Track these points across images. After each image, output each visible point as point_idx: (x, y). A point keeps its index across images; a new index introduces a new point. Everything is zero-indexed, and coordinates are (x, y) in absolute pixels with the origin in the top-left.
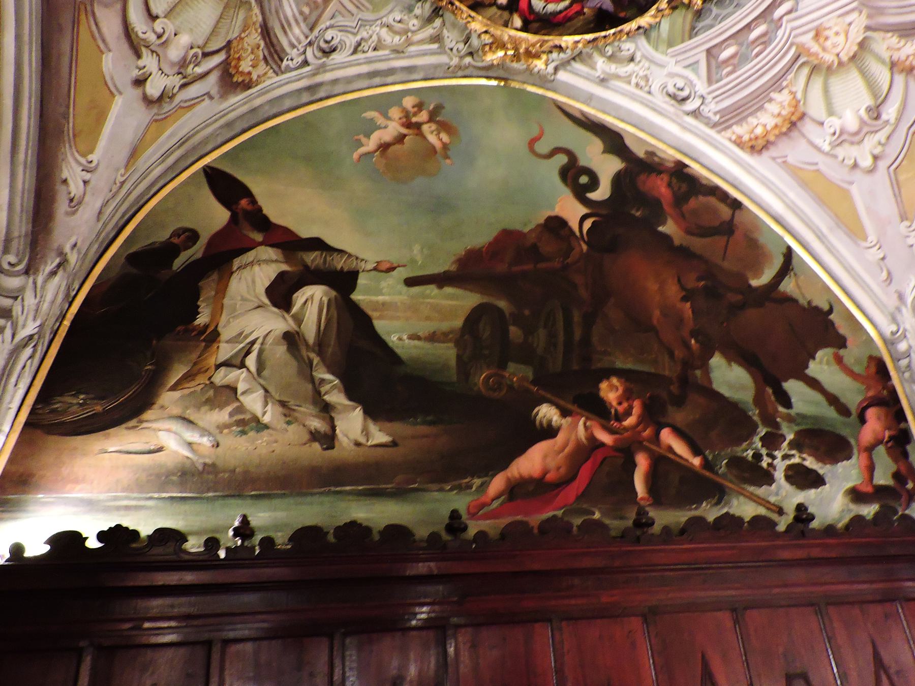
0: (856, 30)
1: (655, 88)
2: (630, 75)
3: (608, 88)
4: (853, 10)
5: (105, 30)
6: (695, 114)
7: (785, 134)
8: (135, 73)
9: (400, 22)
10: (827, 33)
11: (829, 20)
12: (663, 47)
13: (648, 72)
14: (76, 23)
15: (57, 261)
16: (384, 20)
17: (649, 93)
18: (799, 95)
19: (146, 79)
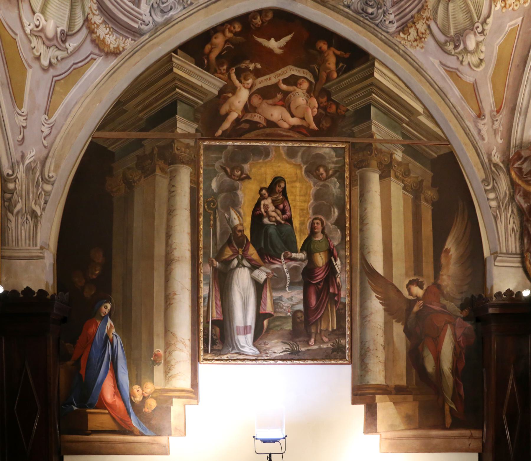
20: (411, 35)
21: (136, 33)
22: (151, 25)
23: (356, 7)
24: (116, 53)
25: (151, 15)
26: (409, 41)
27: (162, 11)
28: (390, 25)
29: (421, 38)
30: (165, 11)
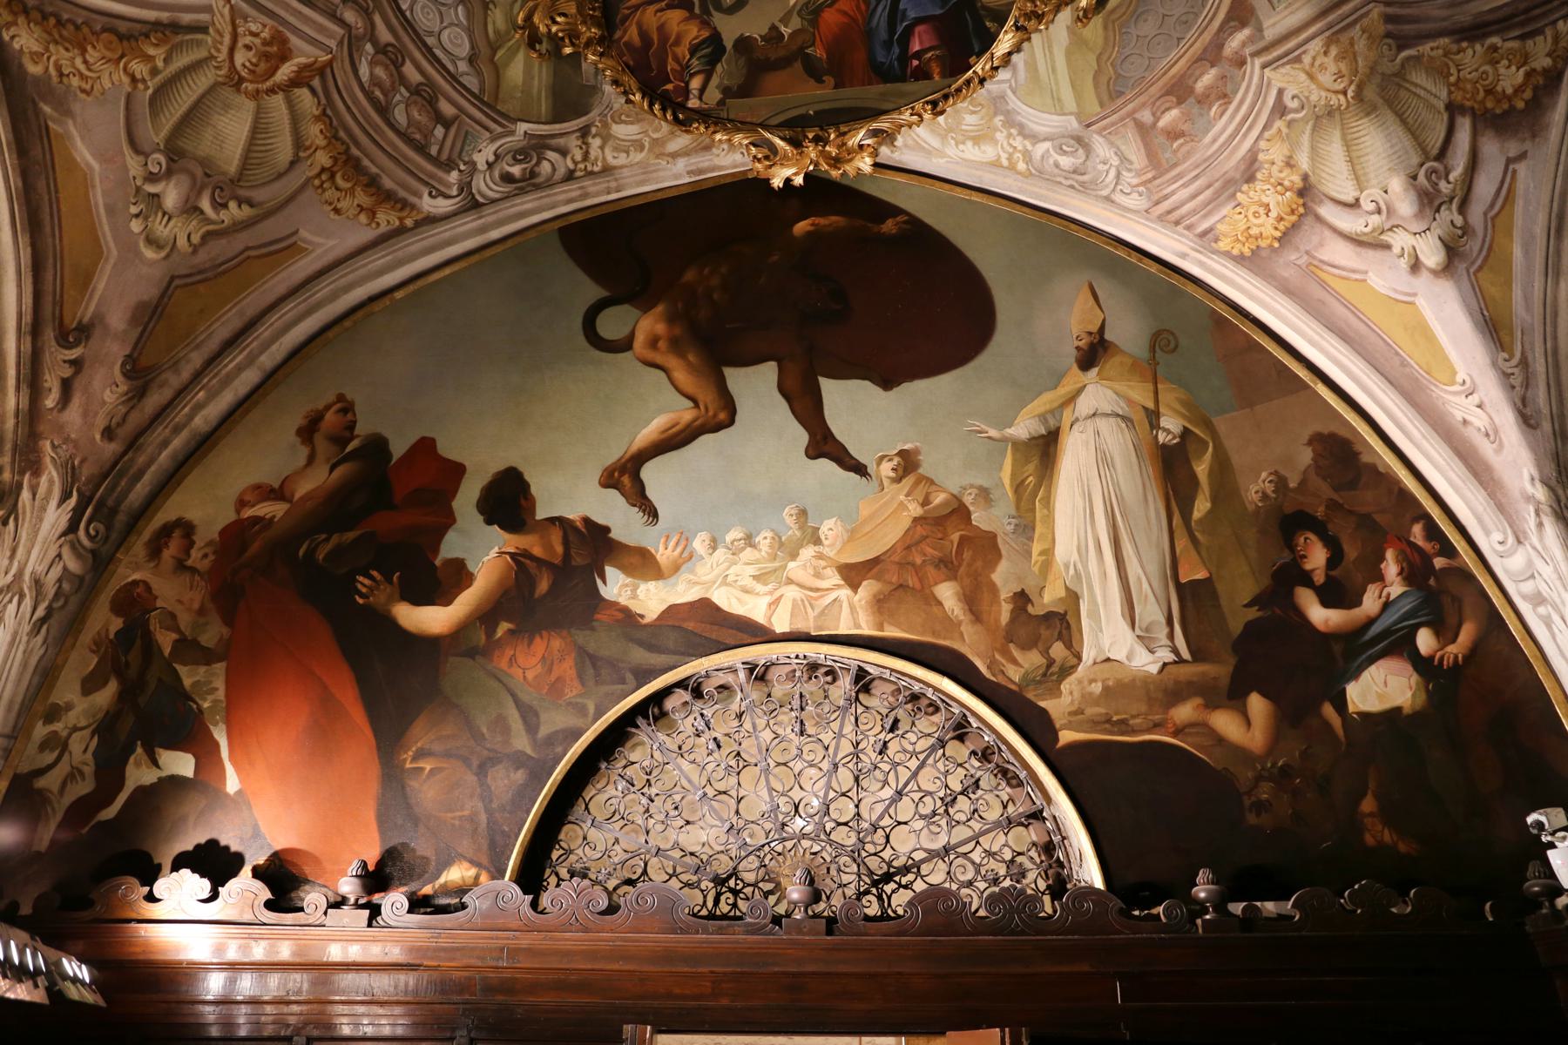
5: (1343, 263)
8: (1404, 264)
14: (1323, 284)
15: (1532, 509)
19: (1417, 257)
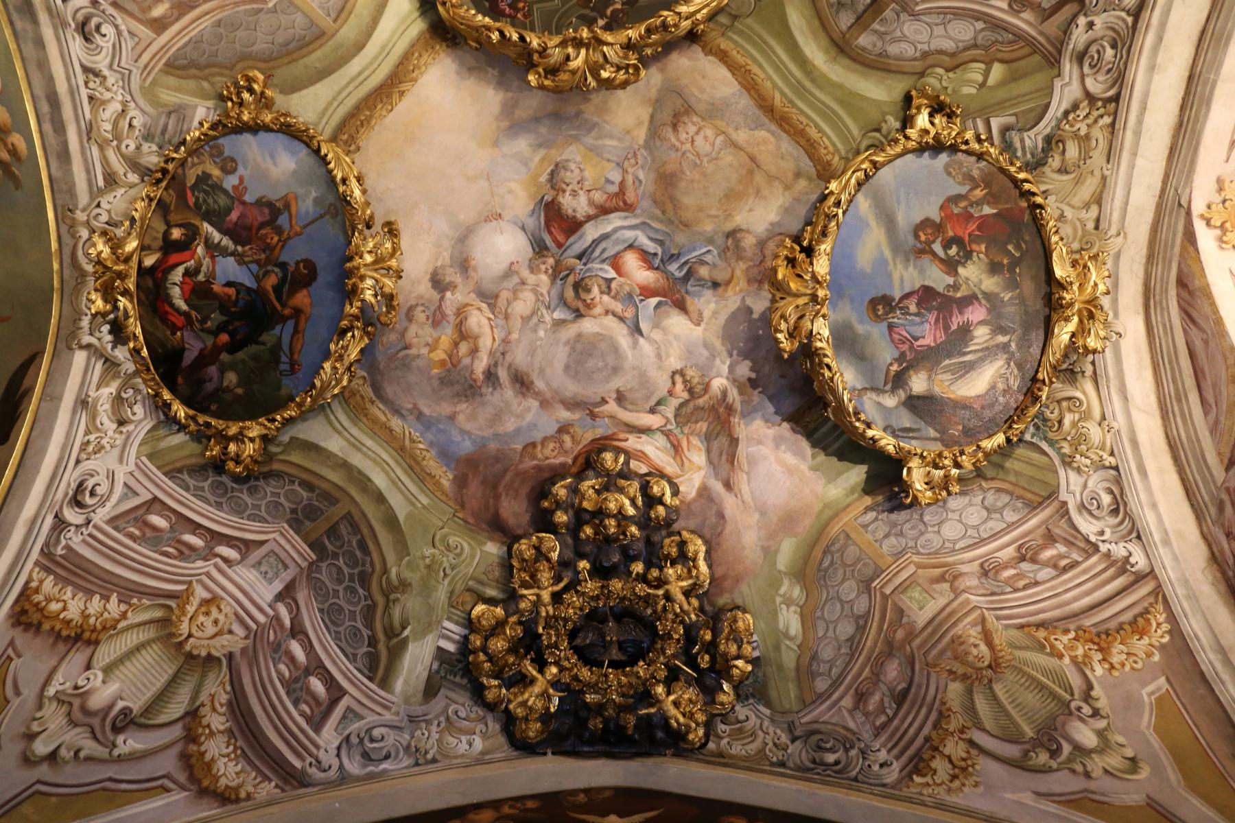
0: (225, 643)
1: (86, 466)
2: (98, 430)
3: (74, 412)
4: (247, 627)
6: (60, 524)
7: (58, 636)
9: (130, 125)
10: (214, 610)
11: (229, 604)
12: (146, 449)
13: (108, 447)
16: (132, 105)
17: (78, 462)
18: (120, 626)
20: (939, 768)
21: (292, 779)
22: (333, 774)
23: (798, 761)
24: (227, 798)
25: (338, 755)
26: (939, 785)
27: (366, 757)
28: (885, 771)
29: (964, 770)
30: (373, 757)
